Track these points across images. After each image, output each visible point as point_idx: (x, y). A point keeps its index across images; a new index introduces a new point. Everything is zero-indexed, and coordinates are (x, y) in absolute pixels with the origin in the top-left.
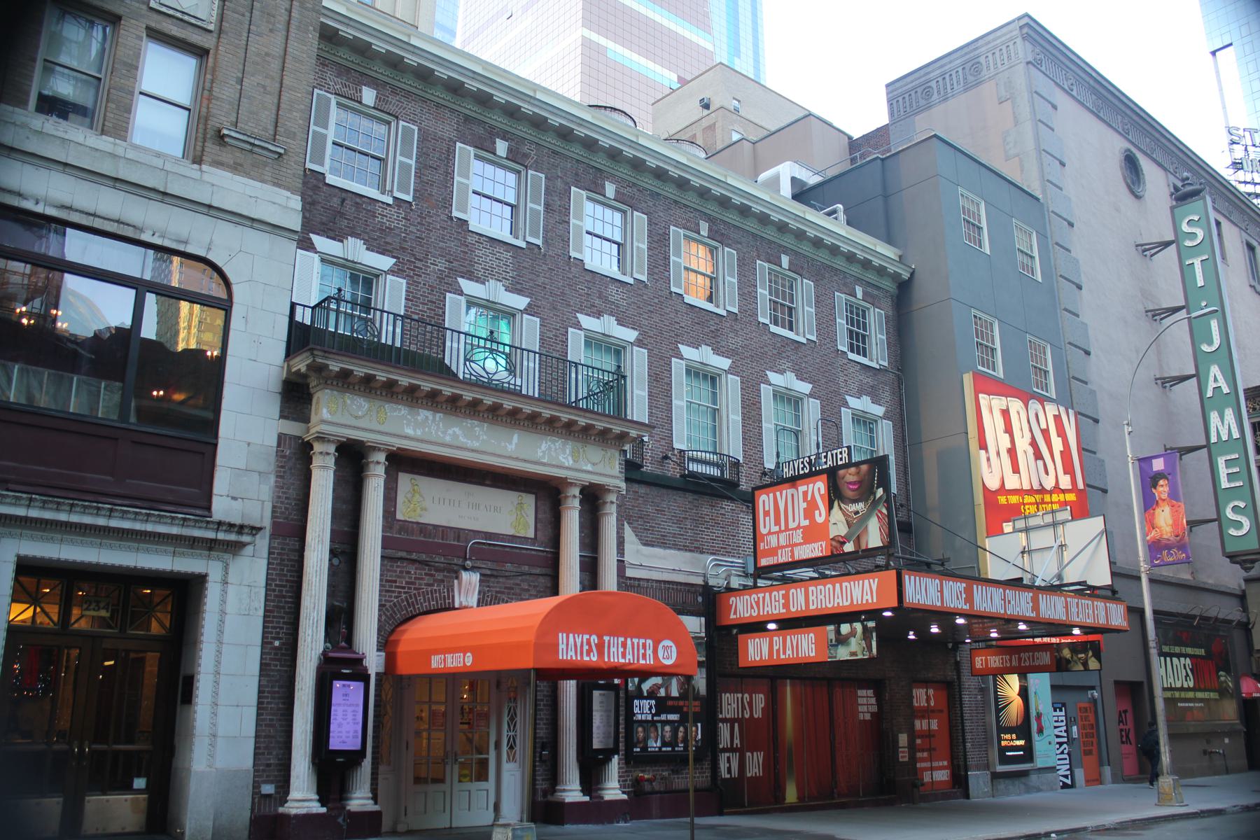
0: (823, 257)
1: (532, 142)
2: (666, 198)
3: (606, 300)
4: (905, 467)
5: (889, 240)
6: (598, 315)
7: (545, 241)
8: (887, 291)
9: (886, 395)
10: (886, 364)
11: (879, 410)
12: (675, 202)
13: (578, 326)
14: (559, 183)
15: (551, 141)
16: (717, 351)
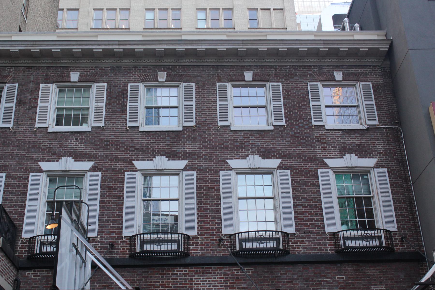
0: (289, 62)
1: (11, 67)
2: (125, 67)
3: (66, 147)
4: (411, 203)
5: (379, 27)
6: (57, 158)
7: (16, 123)
8: (375, 66)
9: (380, 147)
10: (377, 123)
11: (370, 162)
12: (135, 67)
13: (40, 170)
14: (31, 85)
15: (24, 62)
16: (171, 157)
